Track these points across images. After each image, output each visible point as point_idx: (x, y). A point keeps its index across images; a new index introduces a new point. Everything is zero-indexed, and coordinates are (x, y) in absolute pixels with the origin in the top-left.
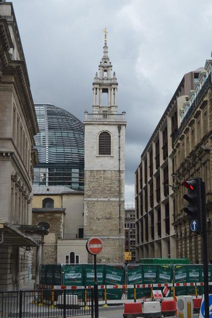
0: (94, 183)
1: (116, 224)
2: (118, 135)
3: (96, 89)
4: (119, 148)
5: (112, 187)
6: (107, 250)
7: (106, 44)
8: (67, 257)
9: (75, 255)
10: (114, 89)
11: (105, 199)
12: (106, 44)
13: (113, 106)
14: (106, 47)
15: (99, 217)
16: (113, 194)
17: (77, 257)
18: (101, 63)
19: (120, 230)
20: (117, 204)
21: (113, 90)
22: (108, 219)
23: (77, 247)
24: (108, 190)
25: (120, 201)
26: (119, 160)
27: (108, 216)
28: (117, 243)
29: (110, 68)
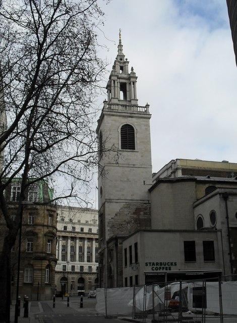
3: (114, 81)
7: (120, 43)
10: (134, 83)
12: (120, 43)
13: (133, 100)
14: (120, 46)
18: (116, 59)
21: (132, 83)
29: (126, 64)
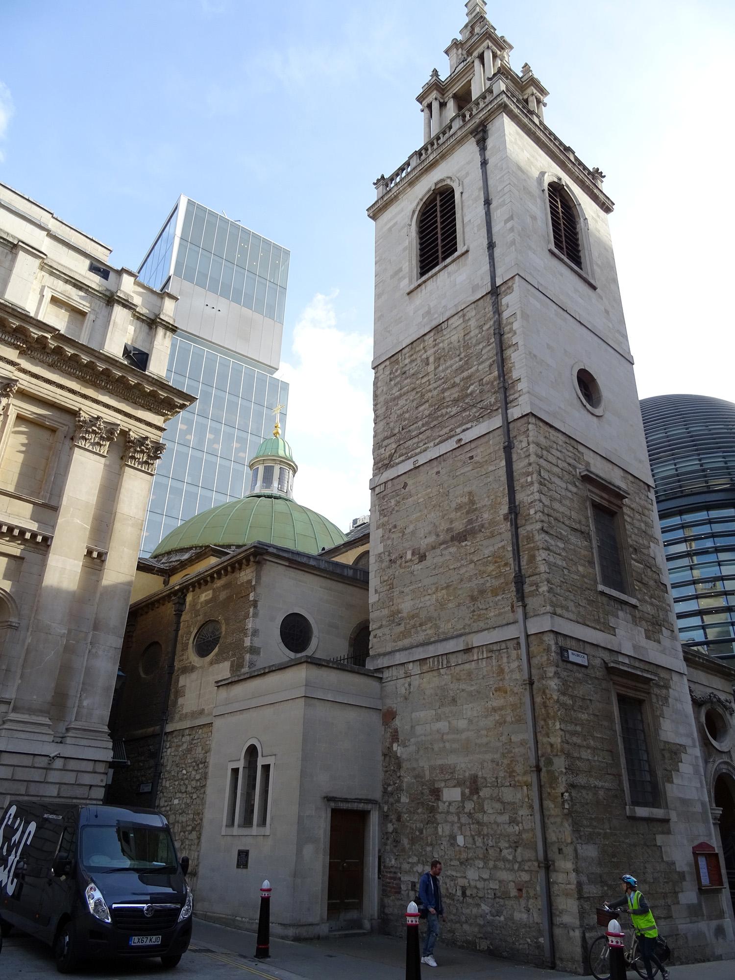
0: (402, 402)
1: (496, 558)
2: (478, 159)
4: (488, 202)
5: (469, 377)
6: (462, 724)
8: (235, 771)
9: (261, 762)
11: (451, 444)
15: (424, 543)
16: (474, 406)
17: (266, 768)
19: (519, 581)
20: (497, 442)
22: (460, 538)
23: (269, 711)
24: (456, 401)
25: (507, 424)
26: (491, 246)
27: (459, 526)
28: (514, 668)
